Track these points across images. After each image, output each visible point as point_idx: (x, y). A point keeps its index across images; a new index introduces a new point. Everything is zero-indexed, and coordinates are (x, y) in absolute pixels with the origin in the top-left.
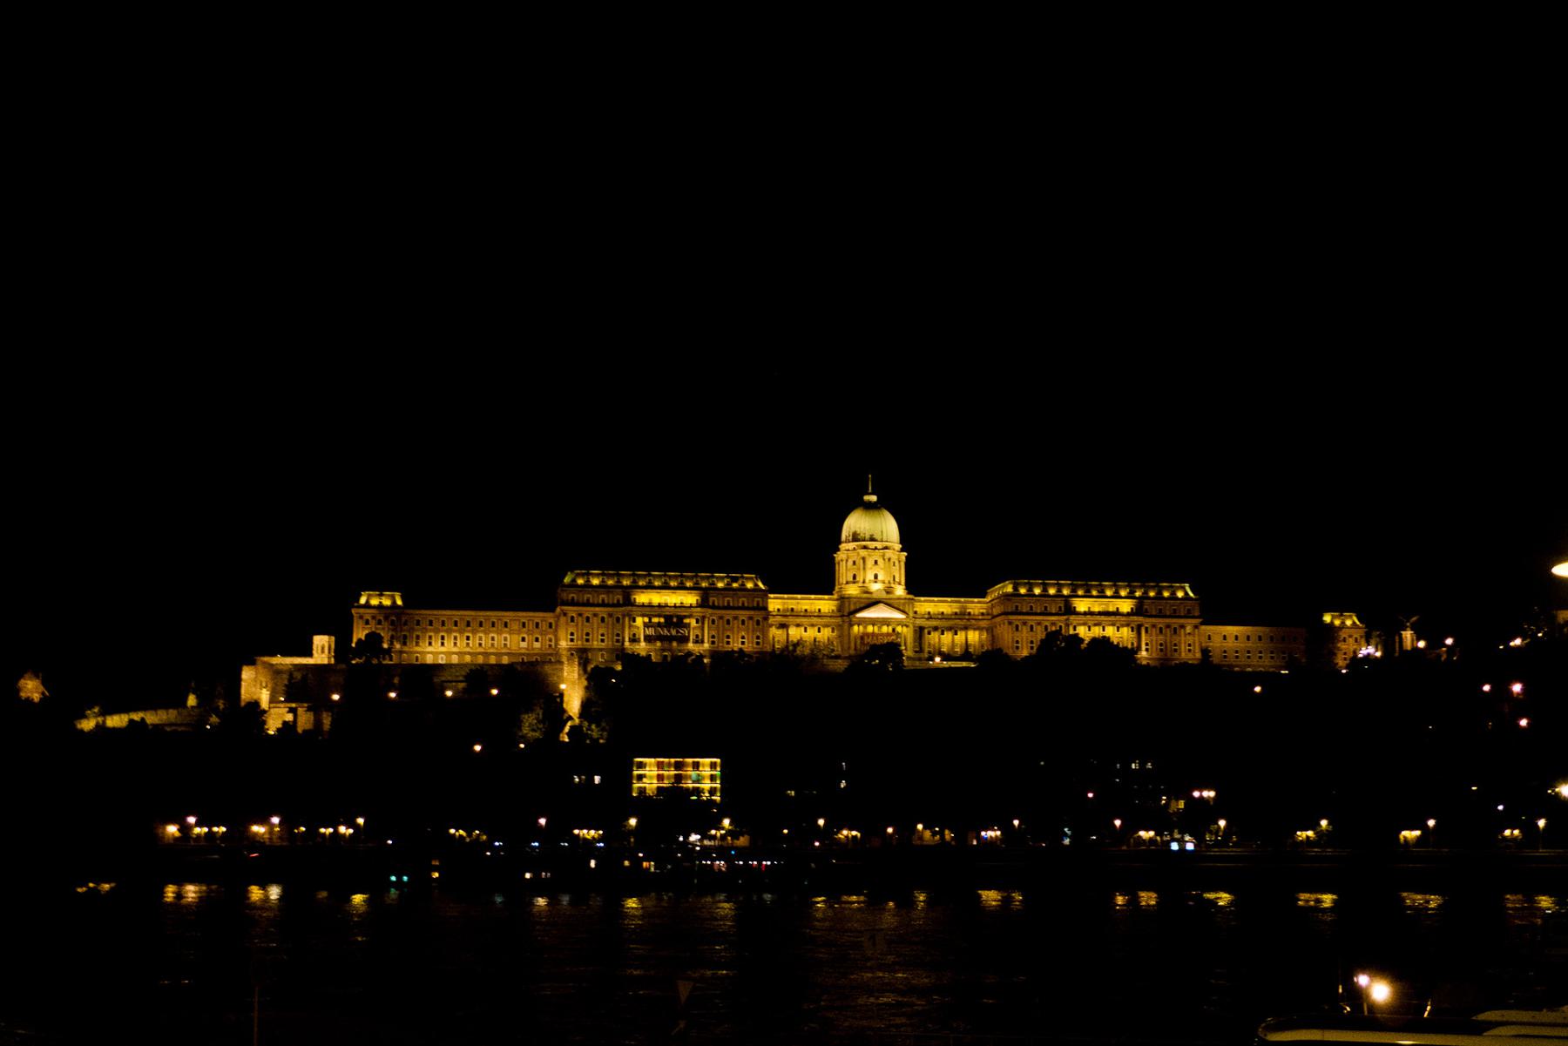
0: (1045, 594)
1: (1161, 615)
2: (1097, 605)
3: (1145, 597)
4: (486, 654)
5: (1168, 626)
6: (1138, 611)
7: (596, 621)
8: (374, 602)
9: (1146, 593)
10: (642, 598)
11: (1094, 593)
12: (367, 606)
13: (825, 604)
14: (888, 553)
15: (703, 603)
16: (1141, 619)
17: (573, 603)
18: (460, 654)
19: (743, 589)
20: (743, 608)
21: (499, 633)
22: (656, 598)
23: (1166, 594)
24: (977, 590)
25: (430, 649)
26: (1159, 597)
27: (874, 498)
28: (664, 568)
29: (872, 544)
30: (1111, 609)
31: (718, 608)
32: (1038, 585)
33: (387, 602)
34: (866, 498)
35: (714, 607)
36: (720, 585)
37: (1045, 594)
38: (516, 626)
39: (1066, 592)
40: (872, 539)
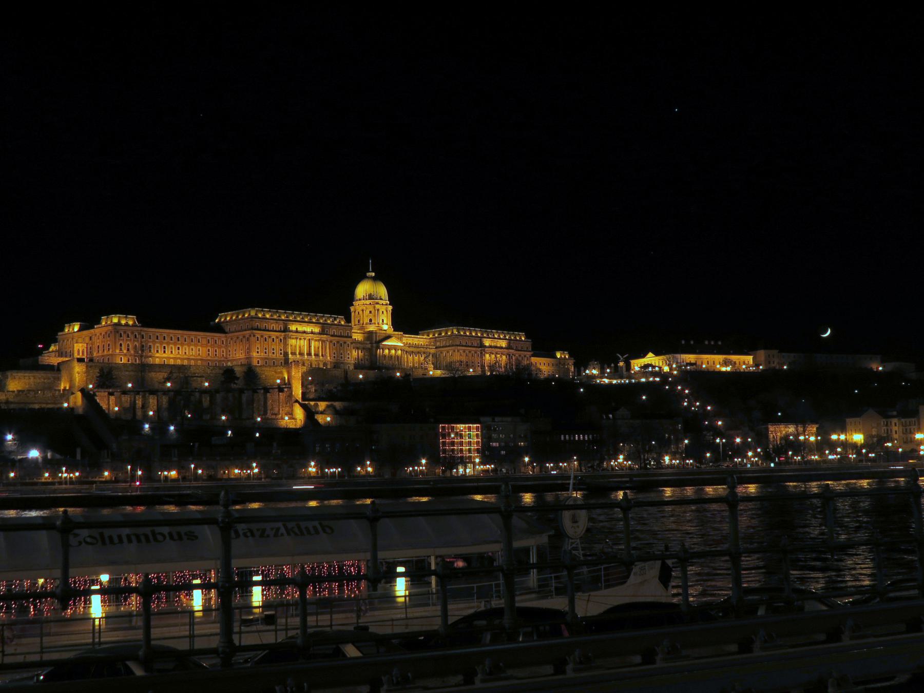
3: (510, 340)
4: (188, 359)
6: (509, 347)
7: (270, 340)
8: (123, 322)
10: (293, 327)
12: (119, 324)
15: (322, 333)
17: (258, 329)
18: (174, 358)
21: (196, 345)
22: (300, 329)
24: (416, 333)
25: (157, 355)
27: (373, 274)
28: (301, 310)
33: (131, 323)
34: (369, 274)
38: (204, 342)
40: (381, 299)
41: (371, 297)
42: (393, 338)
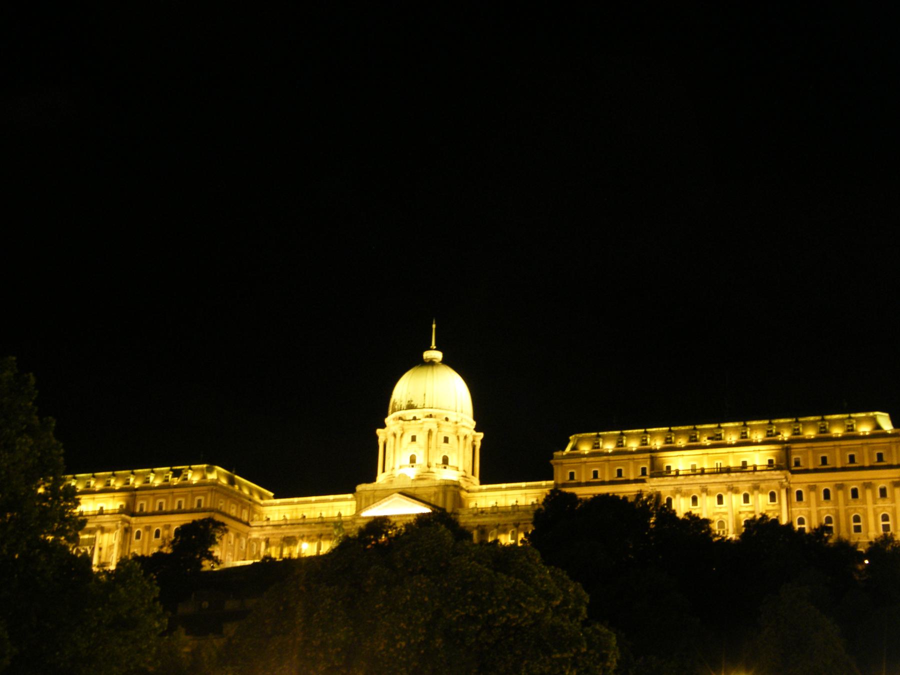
0: (621, 452)
1: (824, 467)
2: (706, 459)
5: (840, 487)
9: (796, 432)
11: (705, 441)
13: (339, 507)
14: (431, 424)
15: (129, 510)
16: (777, 474)
19: (186, 485)
20: (180, 512)
23: (837, 431)
26: (824, 437)
27: (438, 355)
29: (409, 414)
30: (732, 463)
31: (147, 514)
32: (610, 438)
35: (142, 514)
36: (158, 482)
37: (621, 452)
39: (658, 443)
40: (410, 407)
41: (394, 411)
42: (397, 497)
